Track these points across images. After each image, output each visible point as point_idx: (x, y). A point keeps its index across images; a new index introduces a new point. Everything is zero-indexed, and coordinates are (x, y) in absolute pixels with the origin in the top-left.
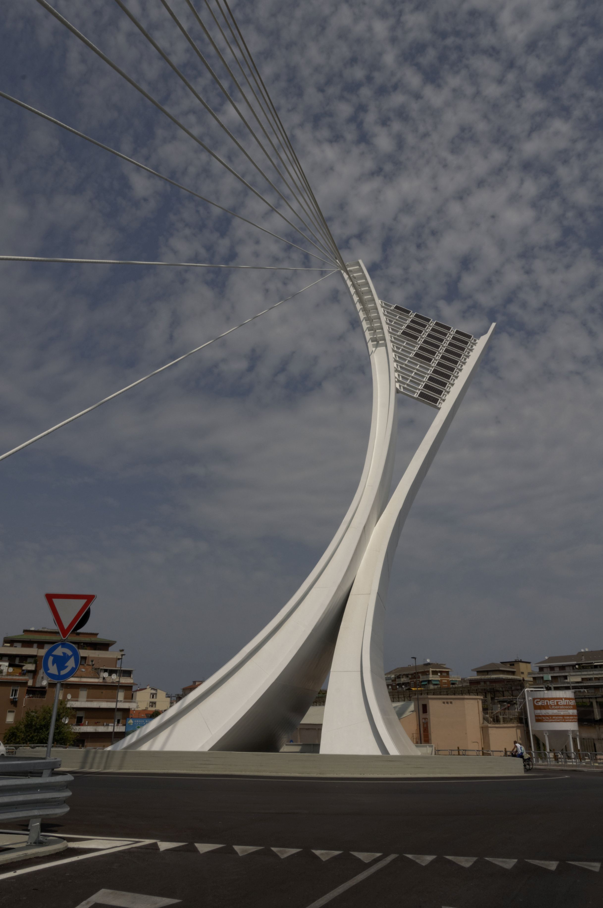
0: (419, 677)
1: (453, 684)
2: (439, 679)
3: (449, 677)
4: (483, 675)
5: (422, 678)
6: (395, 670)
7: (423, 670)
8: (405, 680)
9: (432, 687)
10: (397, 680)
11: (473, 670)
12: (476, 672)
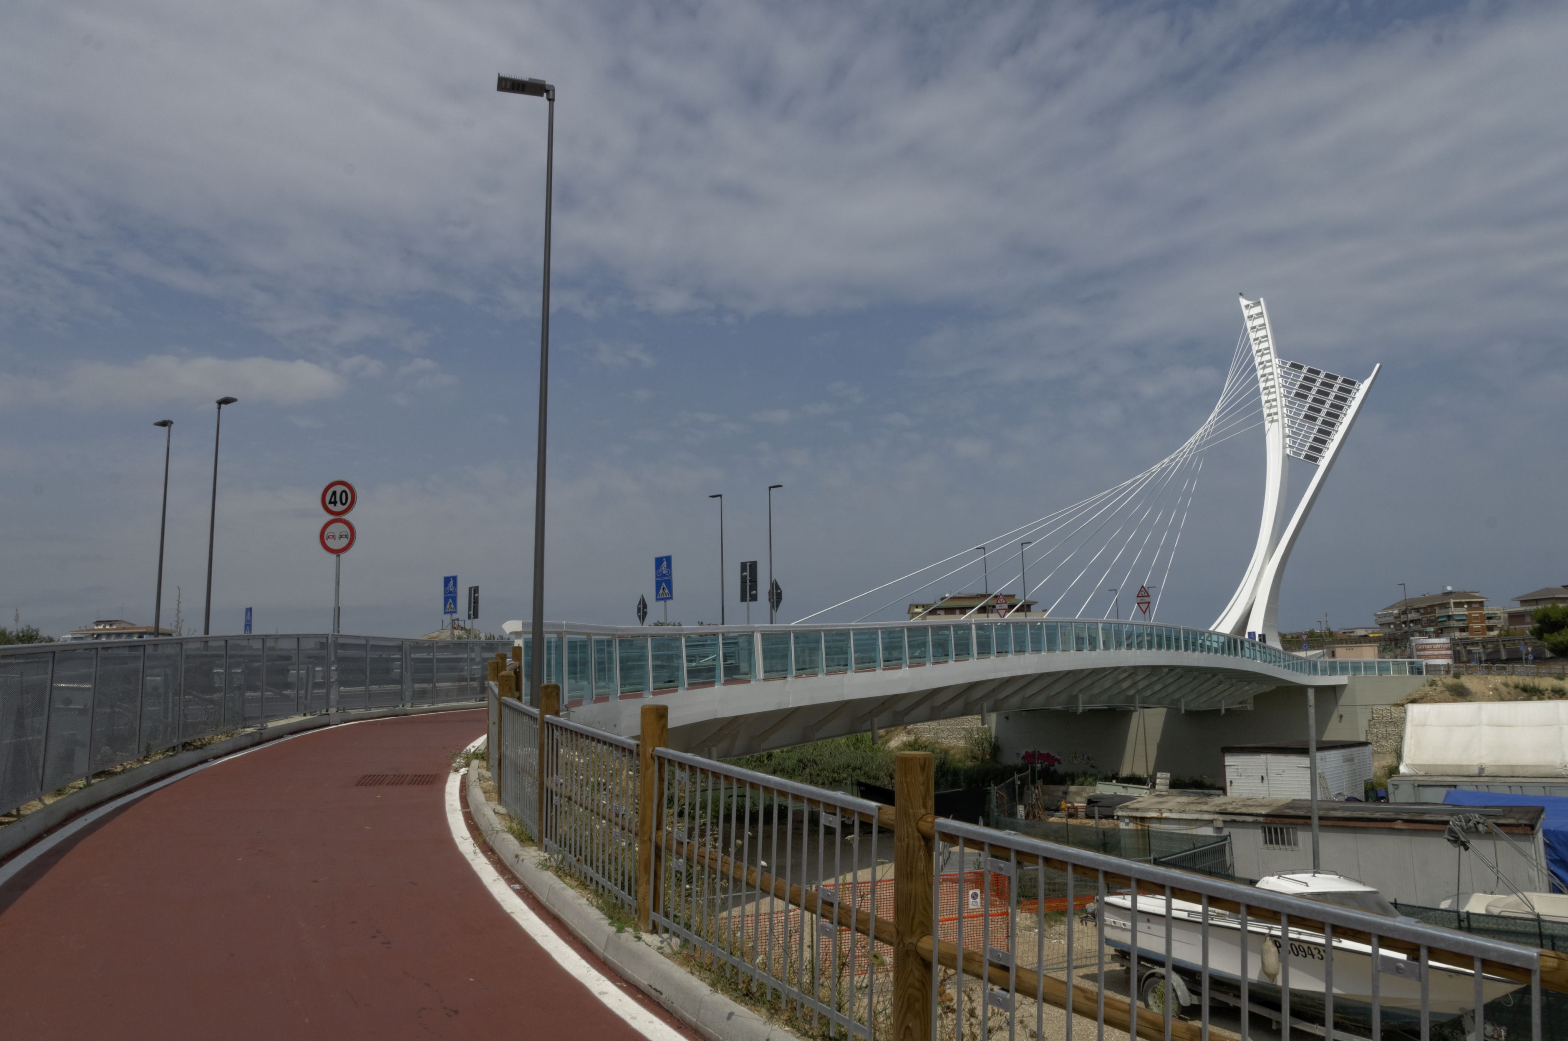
0: (1435, 613)
1: (1489, 618)
2: (1466, 613)
3: (1483, 610)
4: (1530, 605)
5: (1439, 612)
6: (1399, 603)
7: (1440, 602)
8: (1415, 616)
9: (1453, 623)
10: (1402, 616)
11: (1513, 600)
12: (1519, 602)
